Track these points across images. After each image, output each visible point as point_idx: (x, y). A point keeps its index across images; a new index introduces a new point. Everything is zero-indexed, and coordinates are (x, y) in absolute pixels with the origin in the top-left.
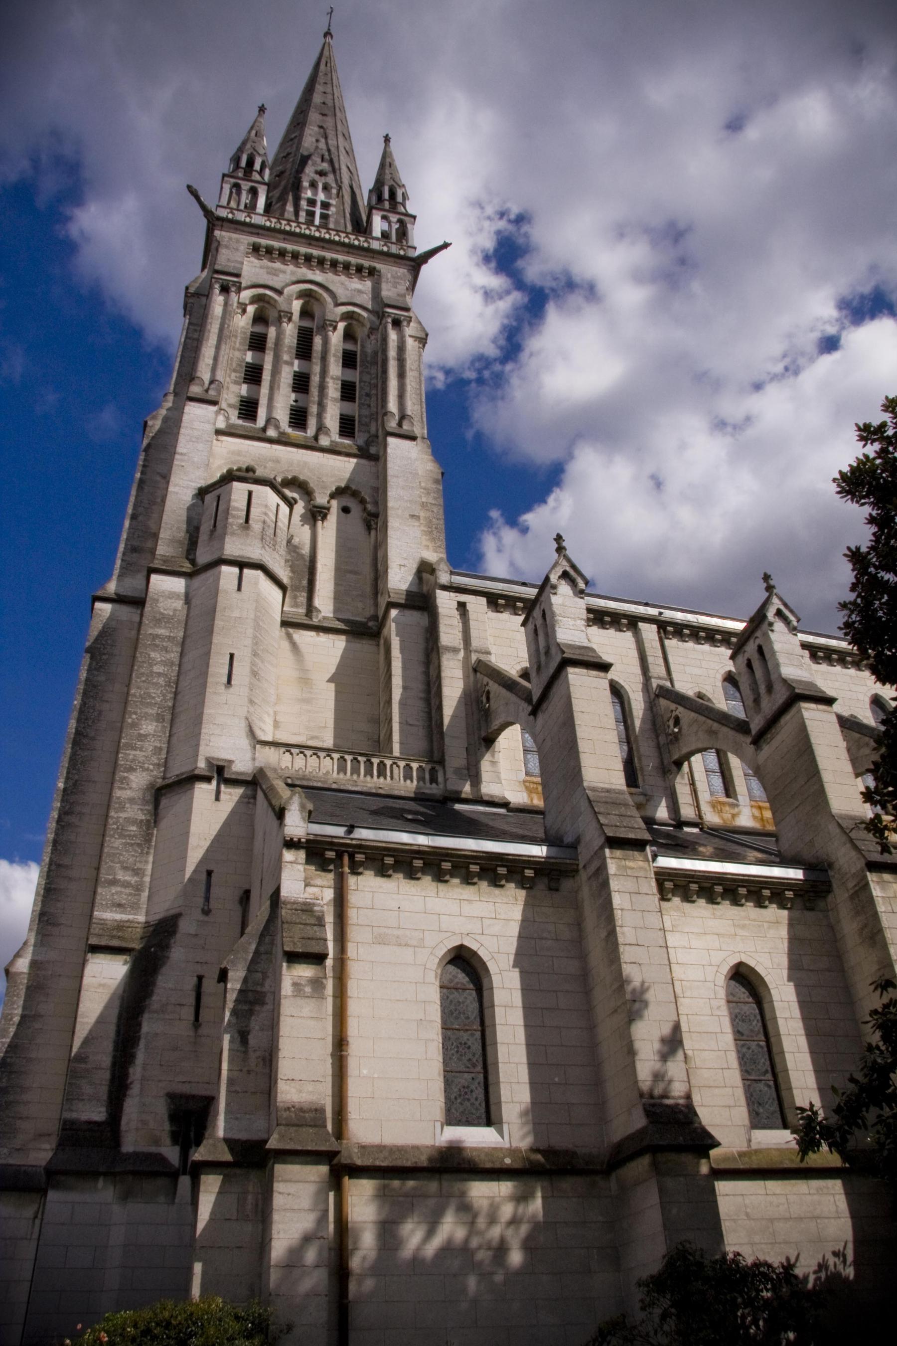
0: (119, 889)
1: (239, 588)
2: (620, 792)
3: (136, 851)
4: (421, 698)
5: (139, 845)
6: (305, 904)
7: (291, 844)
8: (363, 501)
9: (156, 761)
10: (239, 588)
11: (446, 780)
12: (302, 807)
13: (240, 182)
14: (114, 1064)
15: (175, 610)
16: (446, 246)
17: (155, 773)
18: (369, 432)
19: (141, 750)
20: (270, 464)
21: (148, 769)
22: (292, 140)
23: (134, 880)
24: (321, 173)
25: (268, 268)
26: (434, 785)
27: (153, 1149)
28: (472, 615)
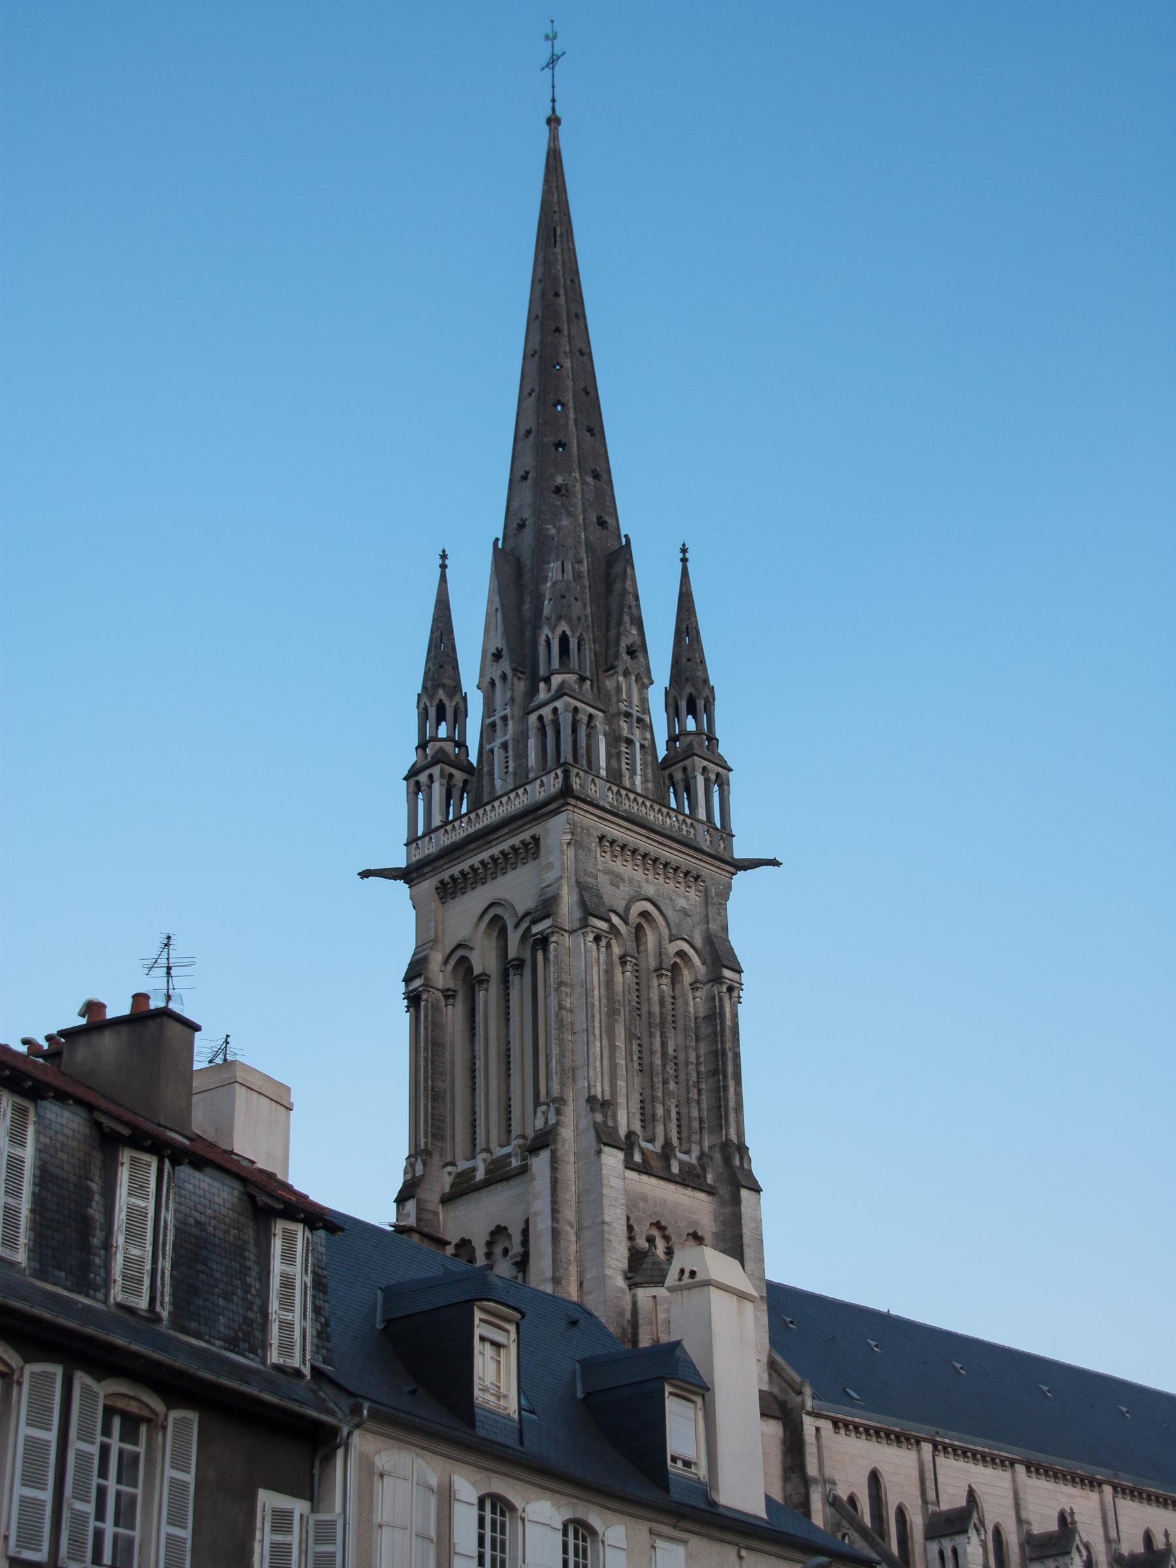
16: (775, 863)
20: (641, 1205)
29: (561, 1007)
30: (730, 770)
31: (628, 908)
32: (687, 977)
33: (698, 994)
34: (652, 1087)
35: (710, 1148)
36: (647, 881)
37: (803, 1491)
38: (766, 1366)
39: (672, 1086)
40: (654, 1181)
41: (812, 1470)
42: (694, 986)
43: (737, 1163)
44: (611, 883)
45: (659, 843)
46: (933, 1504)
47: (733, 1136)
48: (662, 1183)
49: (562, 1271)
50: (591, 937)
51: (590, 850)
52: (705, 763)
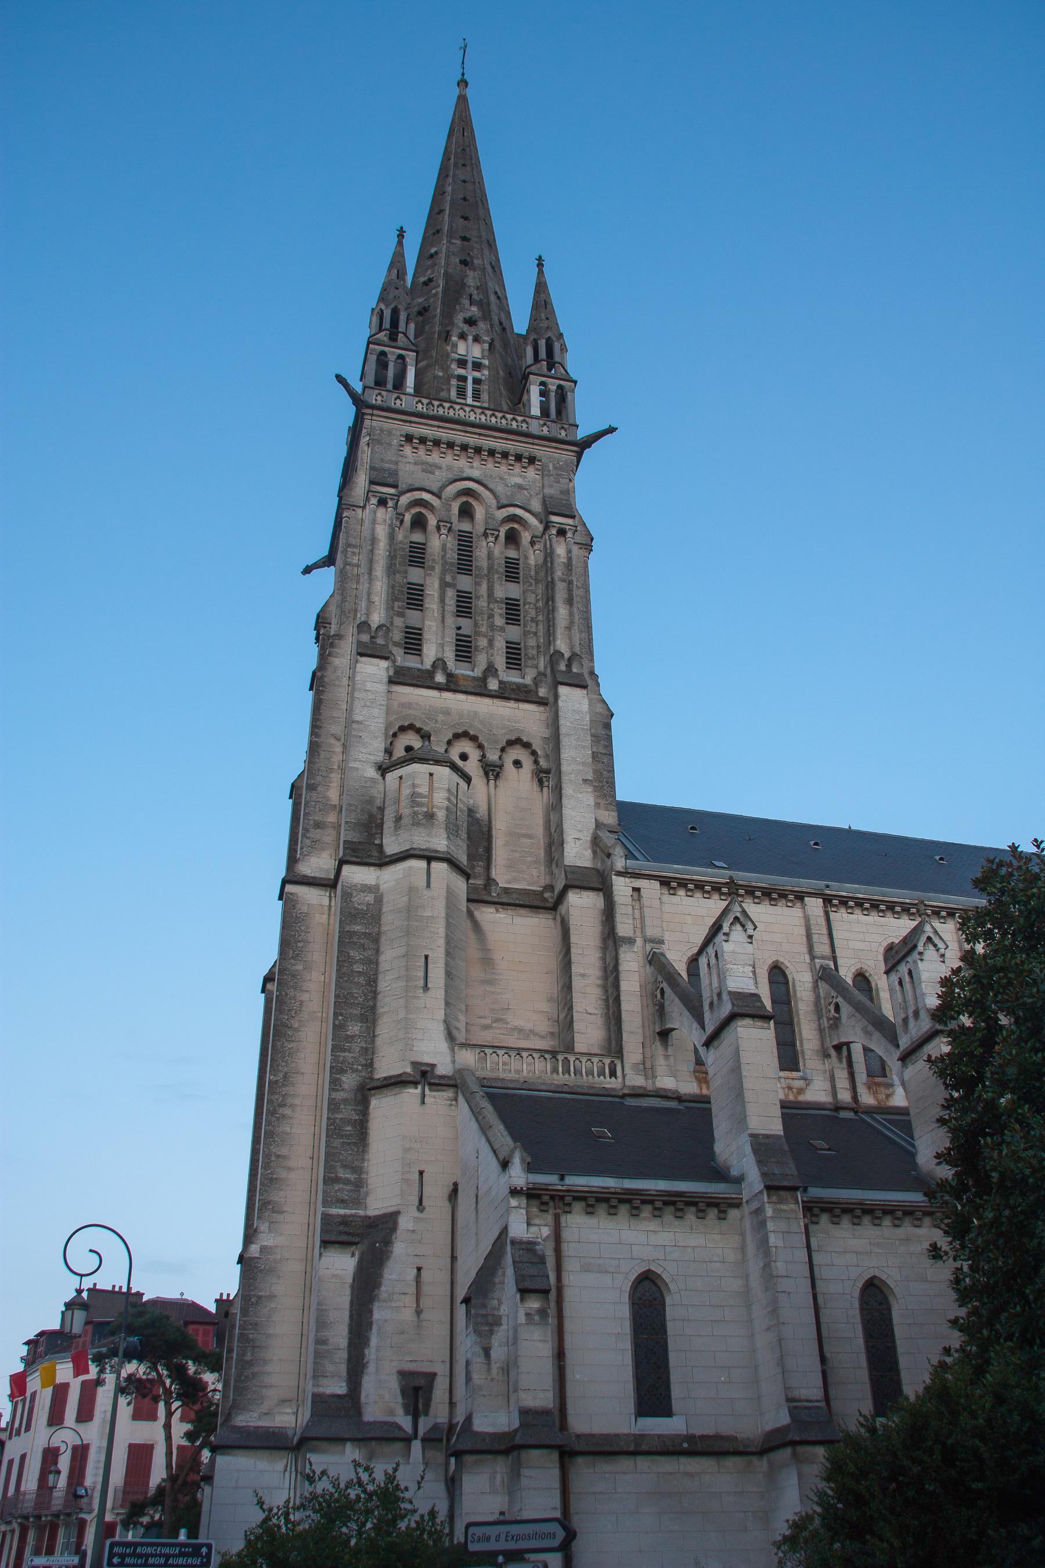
0: (341, 1186)
1: (428, 886)
2: (778, 1137)
3: (353, 1150)
4: (598, 986)
5: (355, 1144)
6: (529, 1243)
7: (514, 1192)
8: (534, 753)
9: (364, 1062)
10: (428, 886)
11: (624, 1076)
12: (523, 1161)
13: (386, 349)
14: (350, 1345)
15: (368, 904)
16: (611, 430)
17: (363, 1074)
18: (537, 667)
19: (350, 1052)
21: (357, 1070)
22: (432, 256)
23: (352, 1177)
24: (471, 322)
25: (423, 463)
26: (613, 1079)
27: (390, 1419)
28: (645, 901)
29: (346, 564)
30: (575, 382)
31: (444, 487)
32: (526, 537)
33: (536, 547)
34: (476, 625)
35: (545, 667)
36: (472, 467)
37: (614, 953)
38: (588, 844)
39: (499, 621)
40: (461, 697)
41: (624, 928)
42: (532, 543)
43: (562, 667)
44: (423, 471)
45: (480, 434)
46: (823, 958)
47: (561, 644)
48: (472, 698)
49: (319, 778)
50: (374, 501)
51: (390, 445)
52: (544, 379)
